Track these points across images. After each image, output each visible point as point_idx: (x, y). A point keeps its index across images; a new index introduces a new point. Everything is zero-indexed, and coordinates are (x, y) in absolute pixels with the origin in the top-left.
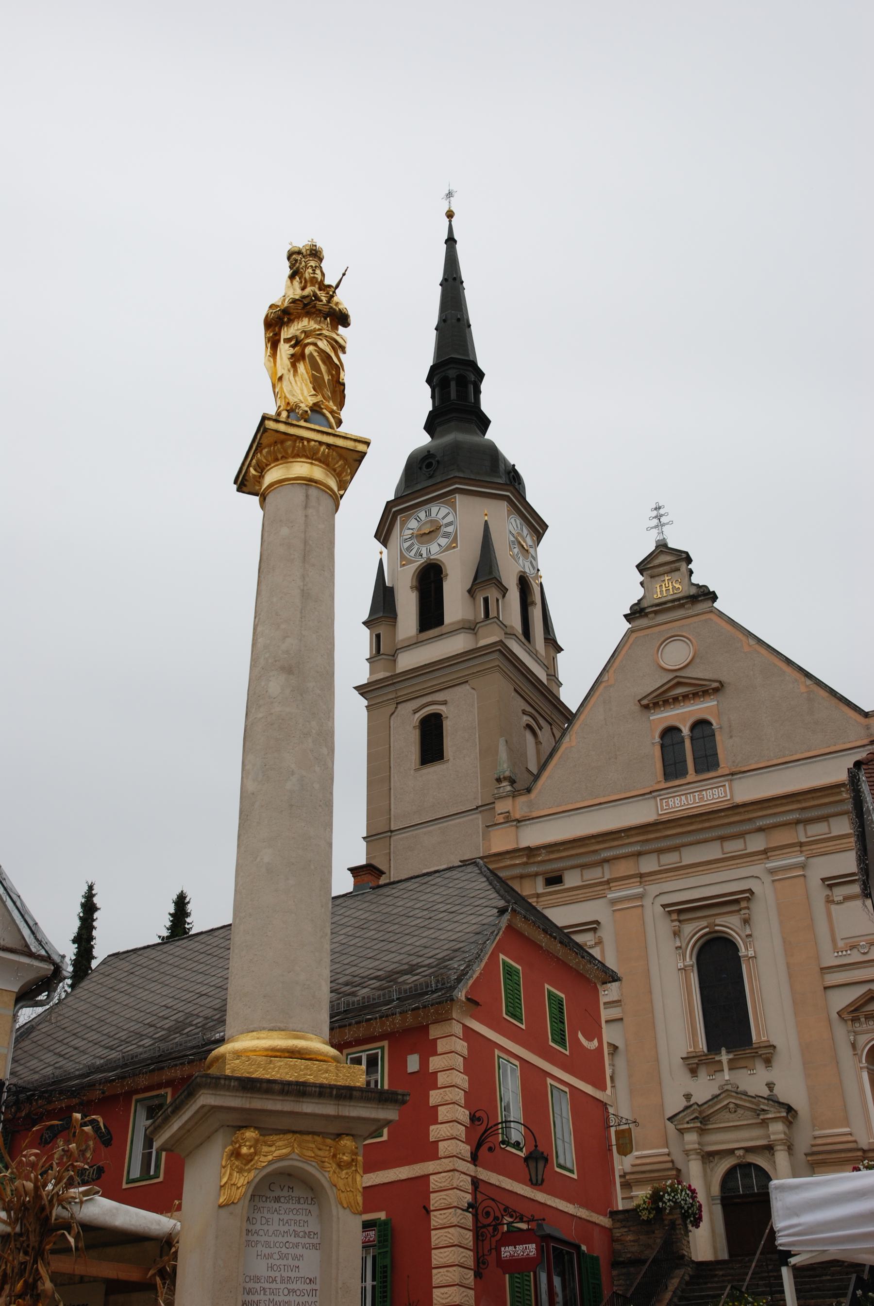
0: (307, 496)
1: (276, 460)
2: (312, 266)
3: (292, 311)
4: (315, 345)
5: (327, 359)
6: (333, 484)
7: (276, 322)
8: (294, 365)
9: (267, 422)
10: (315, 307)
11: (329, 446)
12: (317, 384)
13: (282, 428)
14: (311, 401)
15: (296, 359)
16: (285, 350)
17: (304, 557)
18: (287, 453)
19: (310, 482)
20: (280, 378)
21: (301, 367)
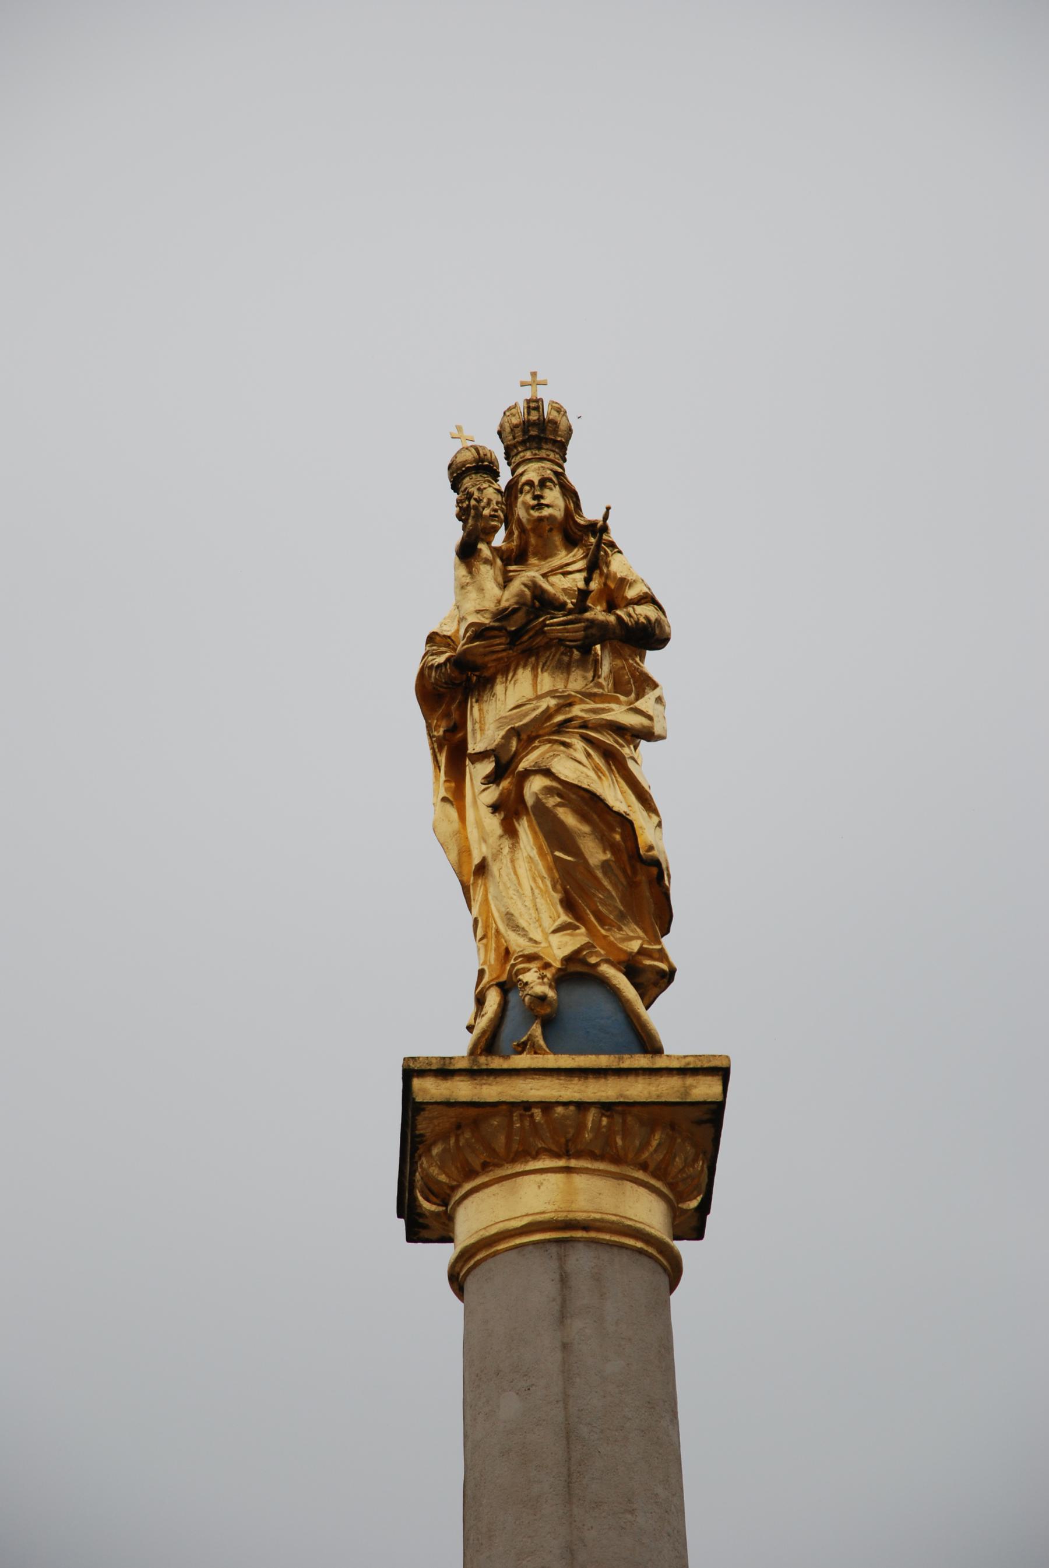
0: (564, 1280)
1: (470, 1174)
2: (530, 483)
3: (479, 660)
4: (547, 773)
5: (589, 804)
6: (646, 1210)
7: (450, 686)
8: (510, 831)
9: (417, 1083)
10: (541, 632)
11: (606, 1107)
12: (575, 895)
13: (463, 1090)
14: (560, 947)
15: (509, 809)
16: (479, 793)
17: (569, 1484)
18: (493, 1151)
19: (564, 1232)
20: (482, 869)
21: (524, 828)
